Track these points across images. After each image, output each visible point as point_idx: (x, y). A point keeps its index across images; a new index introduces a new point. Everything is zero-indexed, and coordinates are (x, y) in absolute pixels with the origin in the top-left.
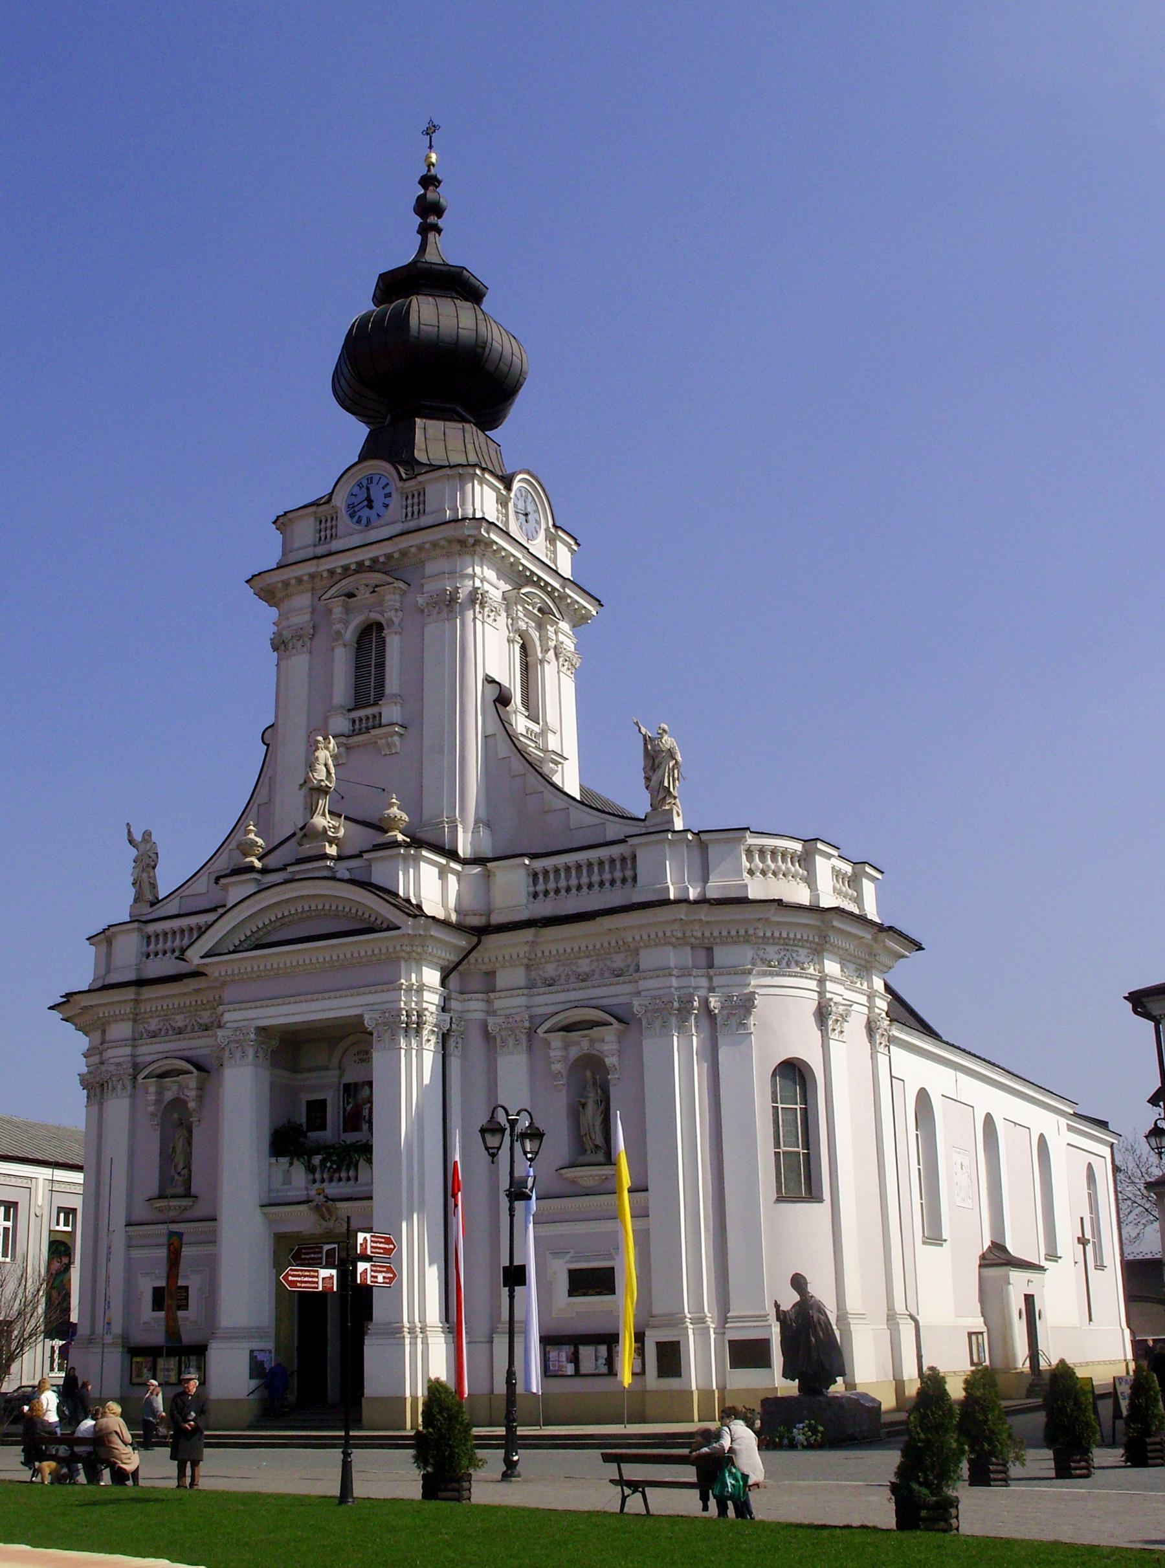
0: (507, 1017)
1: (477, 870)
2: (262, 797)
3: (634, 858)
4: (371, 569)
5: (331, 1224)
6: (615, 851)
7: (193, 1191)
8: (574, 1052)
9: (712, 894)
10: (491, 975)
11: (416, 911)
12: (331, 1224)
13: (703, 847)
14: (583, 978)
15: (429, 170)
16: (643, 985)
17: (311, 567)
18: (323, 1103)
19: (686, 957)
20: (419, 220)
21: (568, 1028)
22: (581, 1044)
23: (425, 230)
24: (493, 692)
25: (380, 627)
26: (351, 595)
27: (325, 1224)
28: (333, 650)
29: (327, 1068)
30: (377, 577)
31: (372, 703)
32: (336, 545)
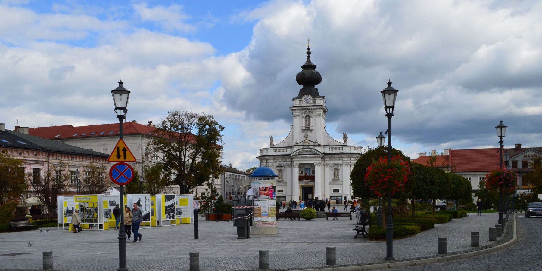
0: (327, 163)
1: (323, 147)
2: (291, 134)
3: (342, 148)
4: (308, 109)
5: (307, 184)
6: (340, 147)
7: (283, 179)
8: (334, 167)
9: (351, 152)
10: (325, 158)
11: (320, 152)
12: (307, 184)
13: (350, 147)
14: (336, 160)
15: (309, 47)
16: (343, 161)
17: (300, 108)
18: (303, 171)
19: (348, 159)
20: (307, 55)
21: (334, 165)
22: (336, 167)
23: (309, 57)
24: (324, 126)
25: (309, 116)
26: (305, 112)
27: (306, 184)
28: (303, 118)
29: (303, 167)
30: (310, 111)
31: (308, 125)
32: (303, 105)
